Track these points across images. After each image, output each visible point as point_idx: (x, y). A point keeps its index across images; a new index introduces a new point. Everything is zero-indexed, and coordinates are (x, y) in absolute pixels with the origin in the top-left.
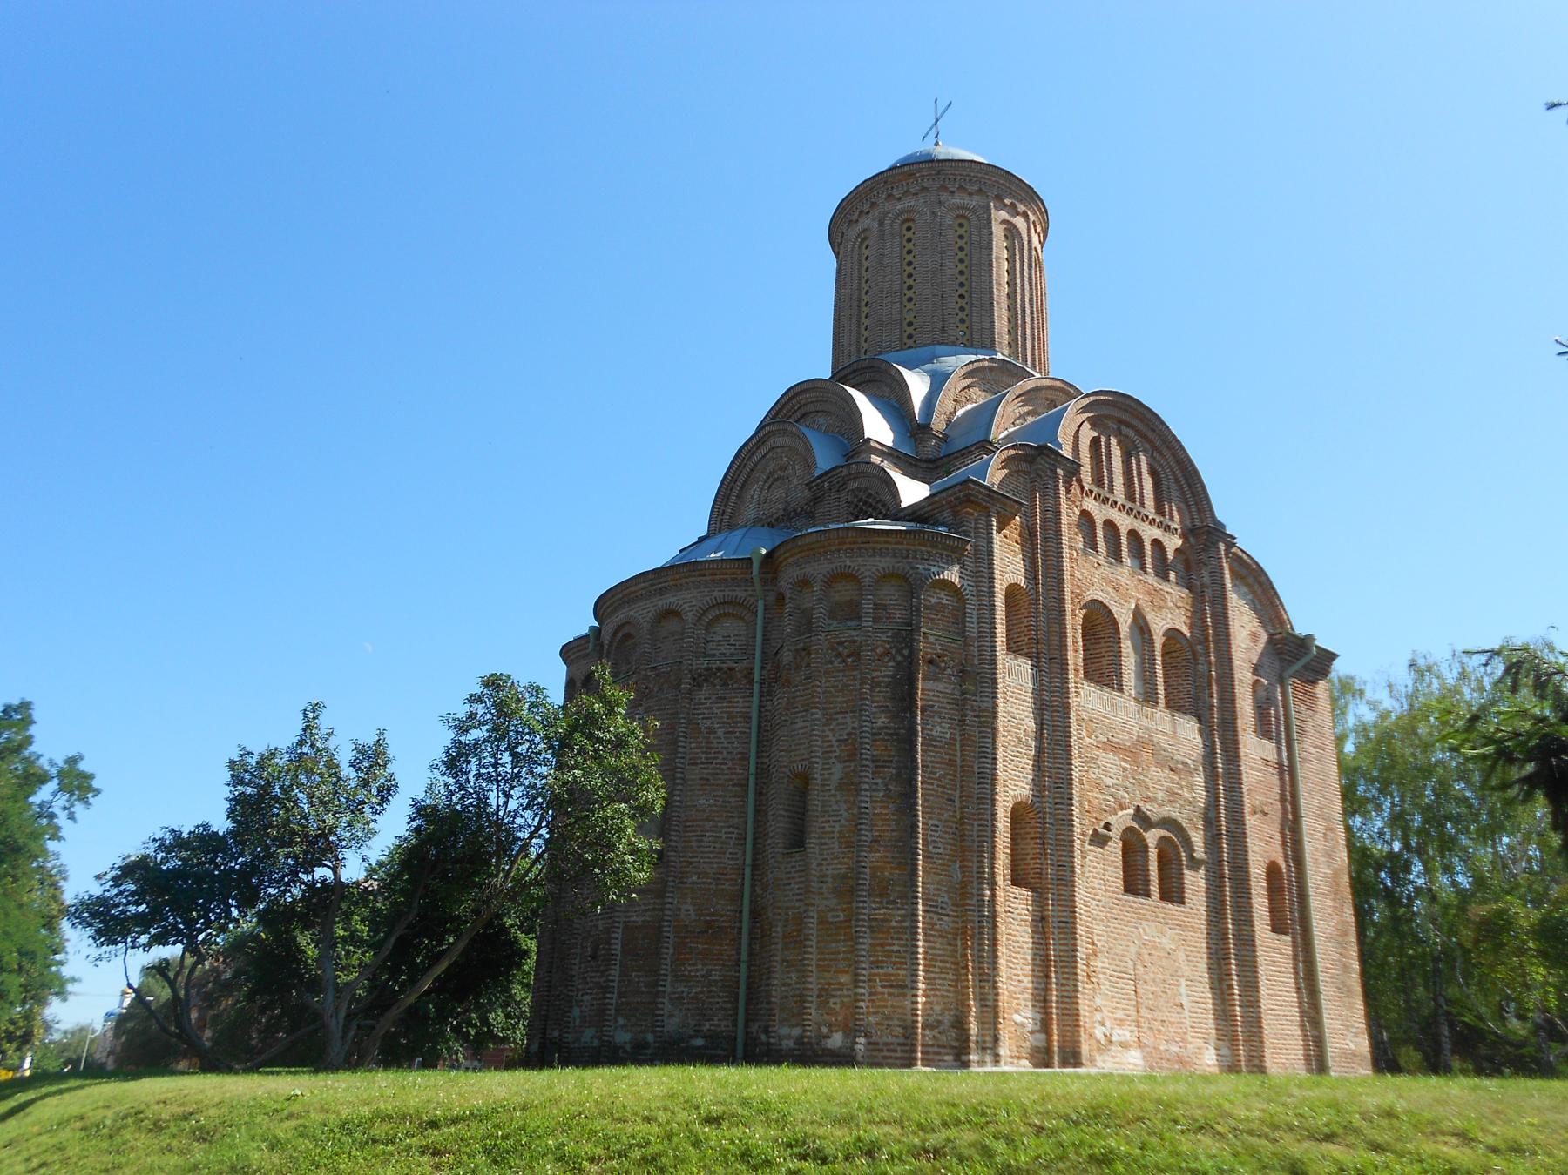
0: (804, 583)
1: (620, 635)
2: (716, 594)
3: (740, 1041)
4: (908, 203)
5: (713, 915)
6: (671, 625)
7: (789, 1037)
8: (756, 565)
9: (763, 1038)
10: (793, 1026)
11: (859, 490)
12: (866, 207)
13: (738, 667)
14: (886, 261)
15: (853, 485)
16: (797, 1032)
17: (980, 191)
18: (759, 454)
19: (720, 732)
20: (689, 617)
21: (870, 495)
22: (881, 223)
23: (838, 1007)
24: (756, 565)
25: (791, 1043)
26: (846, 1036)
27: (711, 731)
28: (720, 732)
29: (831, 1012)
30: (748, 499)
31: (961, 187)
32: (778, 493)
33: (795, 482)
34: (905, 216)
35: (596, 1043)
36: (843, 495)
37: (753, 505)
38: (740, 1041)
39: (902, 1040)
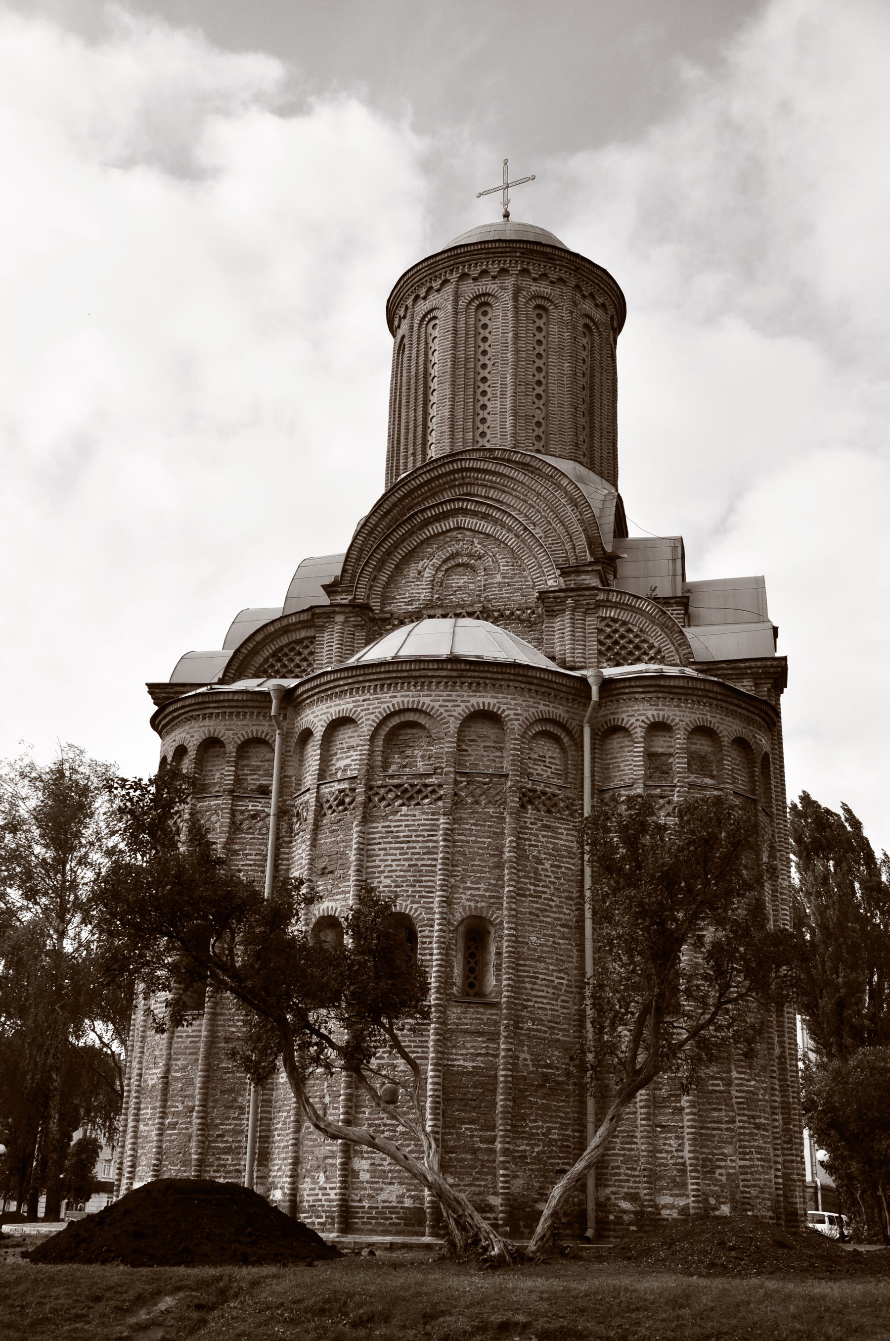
0: (658, 727)
1: (396, 721)
2: (541, 707)
3: (591, 1206)
4: (544, 288)
5: (548, 1066)
6: (484, 729)
7: (672, 1207)
8: (595, 689)
9: (625, 1205)
10: (677, 1196)
11: (615, 620)
12: (494, 269)
13: (562, 794)
14: (521, 344)
15: (603, 613)
16: (682, 1202)
17: (603, 305)
18: (437, 528)
19: (547, 865)
20: (515, 726)
21: (630, 631)
22: (515, 298)
23: (724, 1179)
24: (595, 689)
25: (675, 1214)
26: (733, 1209)
27: (539, 861)
28: (547, 865)
29: (716, 1182)
30: (413, 573)
31: (592, 295)
32: (459, 580)
33: (498, 578)
34: (539, 302)
35: (408, 1203)
36: (591, 620)
37: (424, 583)
38: (591, 1206)
39: (770, 1214)
